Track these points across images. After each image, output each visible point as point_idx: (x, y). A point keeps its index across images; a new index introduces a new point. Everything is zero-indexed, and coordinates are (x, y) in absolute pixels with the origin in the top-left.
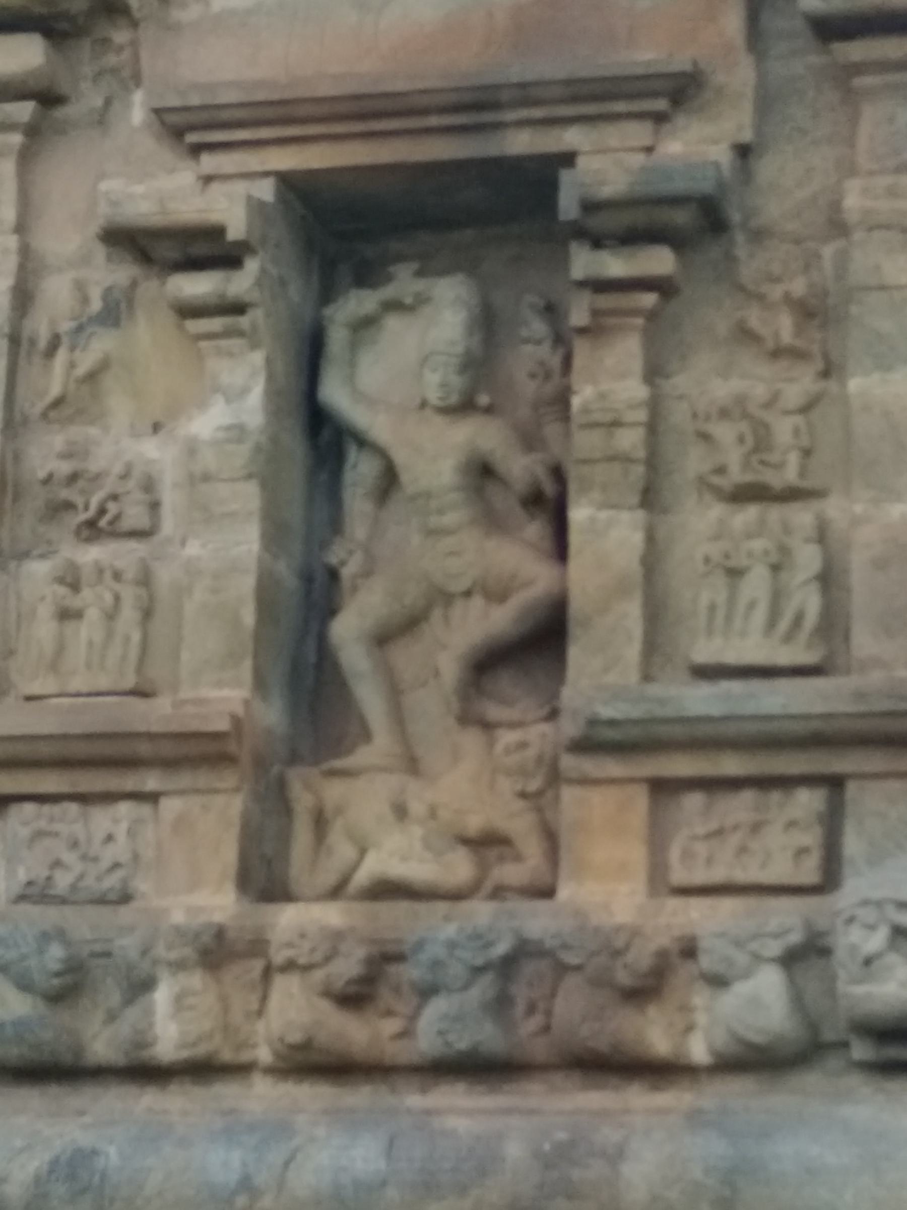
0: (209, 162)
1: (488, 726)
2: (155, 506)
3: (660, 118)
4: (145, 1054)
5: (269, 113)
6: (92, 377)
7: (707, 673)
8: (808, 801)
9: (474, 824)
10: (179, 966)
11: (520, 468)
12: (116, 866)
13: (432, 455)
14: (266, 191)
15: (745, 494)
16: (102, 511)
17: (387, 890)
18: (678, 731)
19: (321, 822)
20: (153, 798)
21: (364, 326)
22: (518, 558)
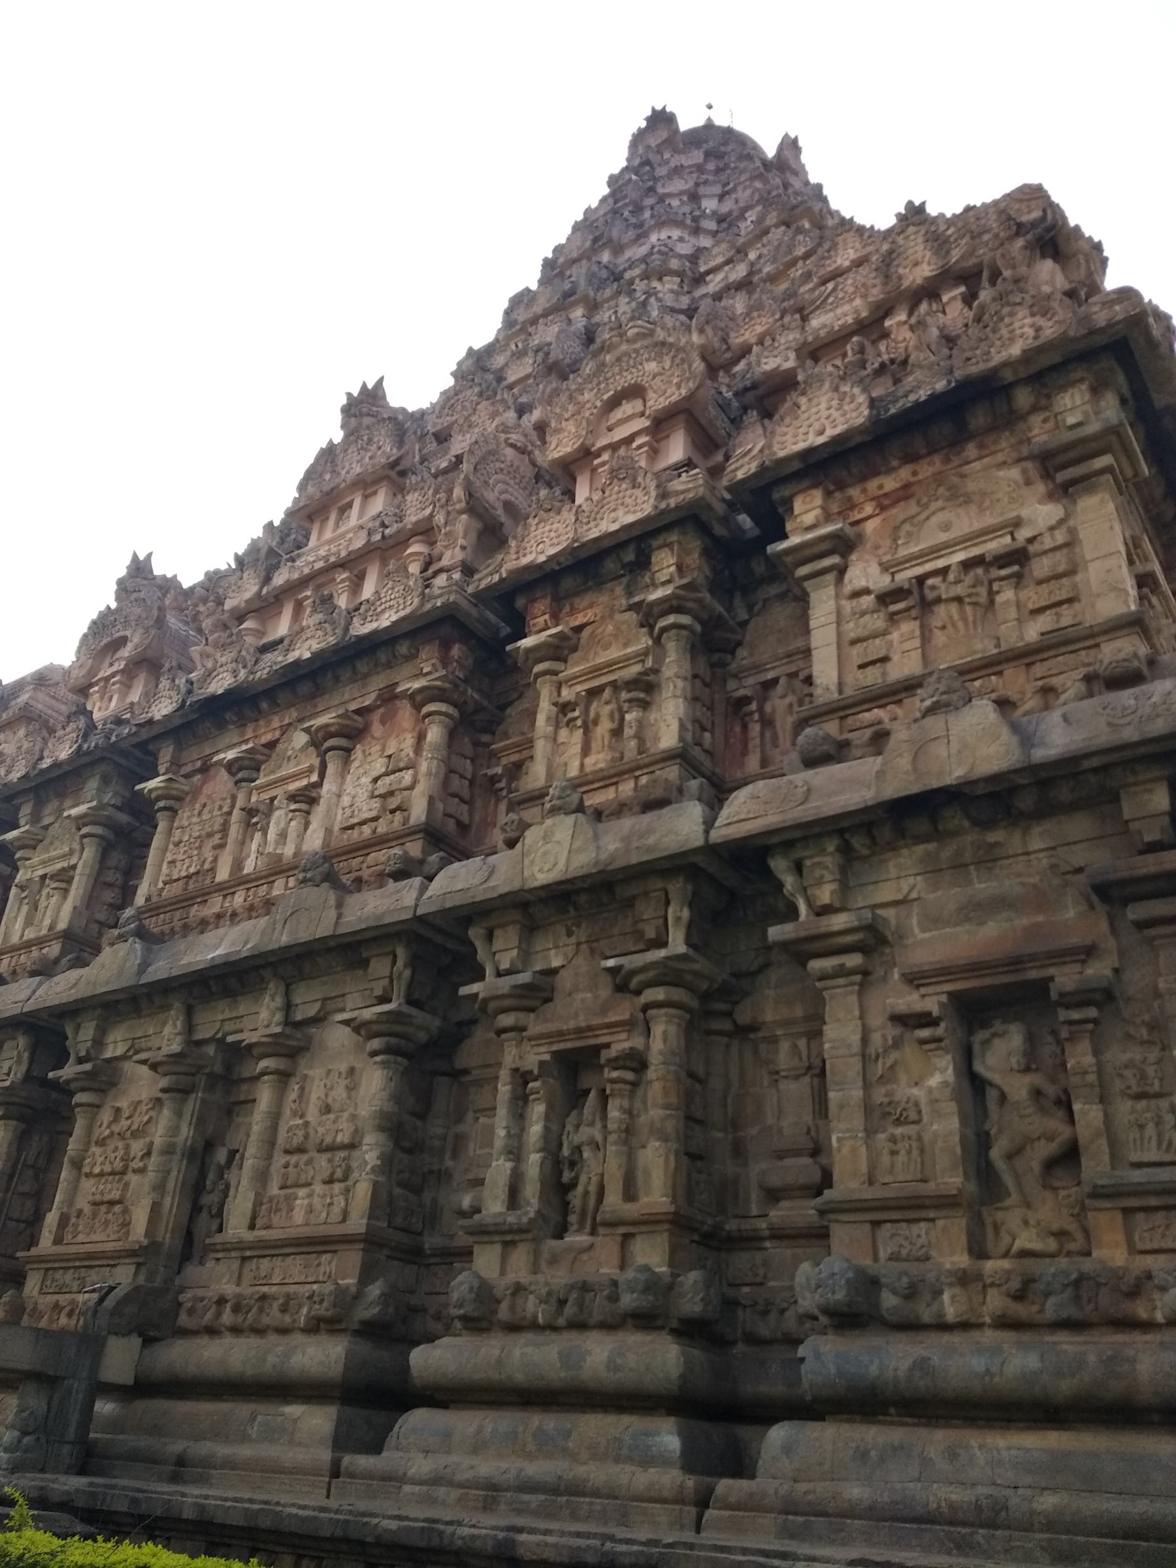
0: (923, 990)
1: (1055, 1189)
9: (1055, 1227)
11: (1051, 1090)
13: (1018, 1088)
15: (1139, 1097)
17: (1025, 1254)
19: (996, 1227)
21: (986, 1043)
22: (1055, 1123)
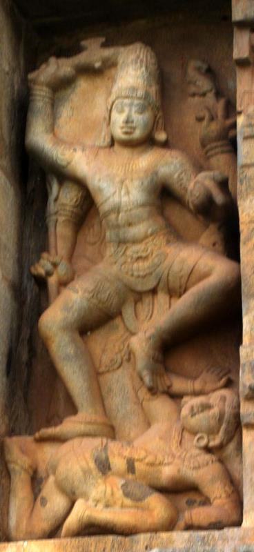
1: (176, 397)
9: (167, 473)
11: (196, 185)
13: (119, 182)
19: (36, 481)
21: (61, 86)
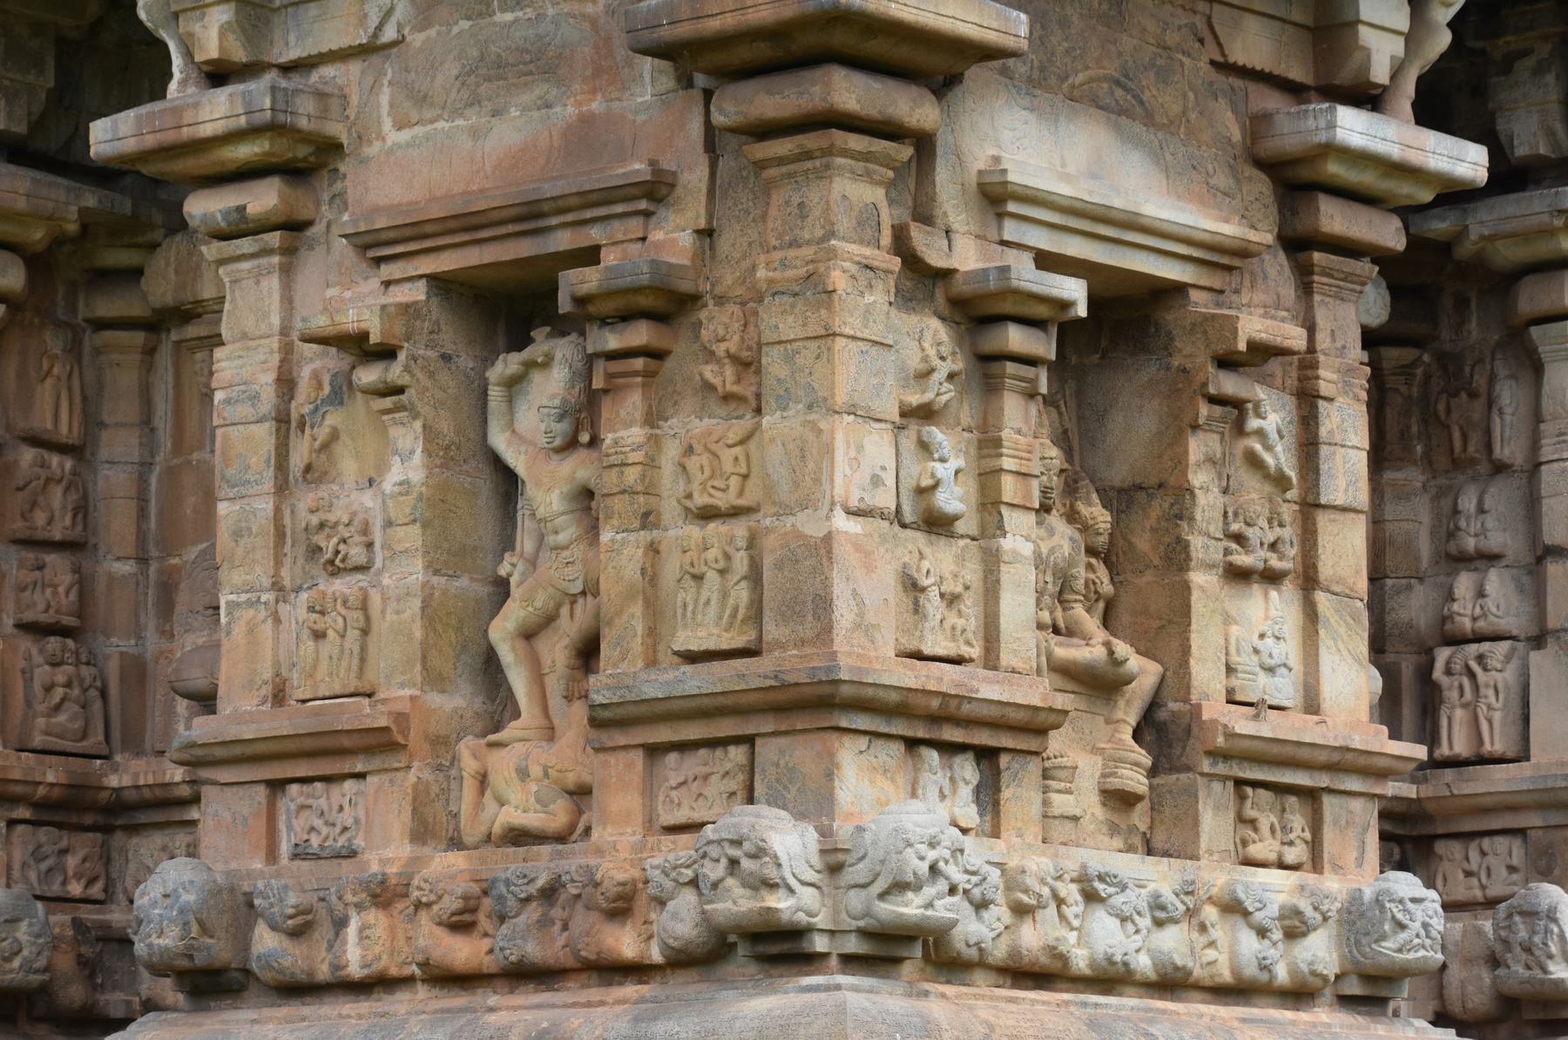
0: (388, 271)
2: (370, 545)
3: (647, 214)
4: (342, 973)
5: (408, 232)
6: (325, 447)
7: (692, 658)
8: (737, 754)
9: (571, 779)
10: (359, 907)
12: (345, 829)
14: (417, 293)
15: (707, 515)
16: (338, 552)
17: (519, 837)
18: (643, 710)
20: (361, 776)
21: (514, 384)
